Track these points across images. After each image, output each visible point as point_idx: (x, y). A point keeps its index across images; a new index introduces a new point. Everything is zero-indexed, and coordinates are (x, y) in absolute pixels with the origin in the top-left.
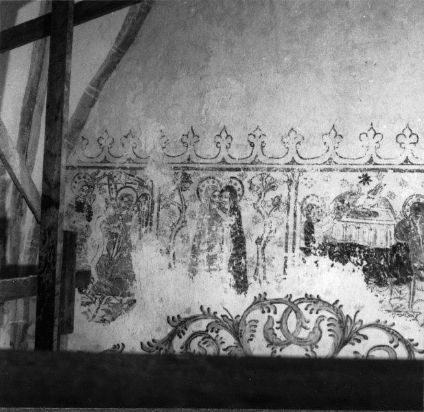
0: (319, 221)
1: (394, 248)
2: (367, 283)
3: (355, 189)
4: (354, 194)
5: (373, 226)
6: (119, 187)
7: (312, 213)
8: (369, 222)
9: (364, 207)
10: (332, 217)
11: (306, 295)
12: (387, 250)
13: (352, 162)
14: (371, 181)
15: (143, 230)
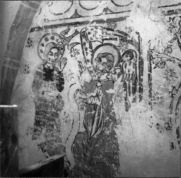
6: (94, 45)
15: (130, 98)
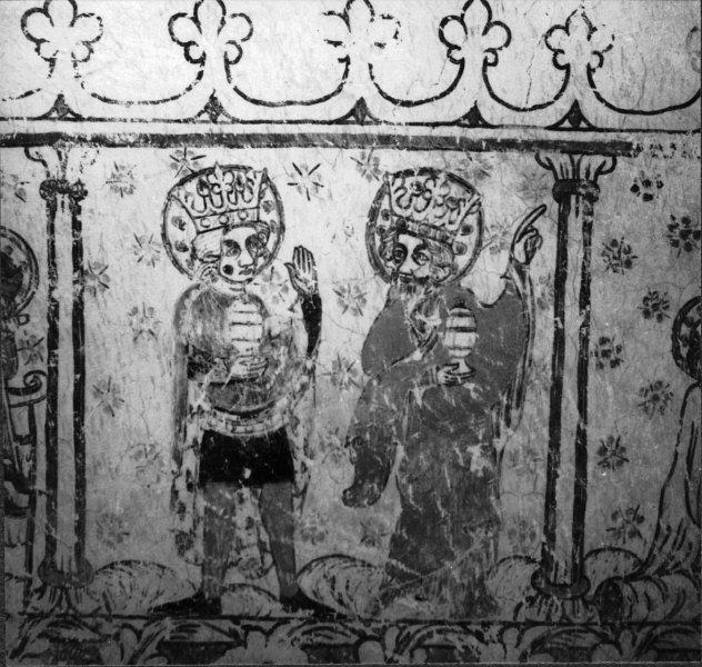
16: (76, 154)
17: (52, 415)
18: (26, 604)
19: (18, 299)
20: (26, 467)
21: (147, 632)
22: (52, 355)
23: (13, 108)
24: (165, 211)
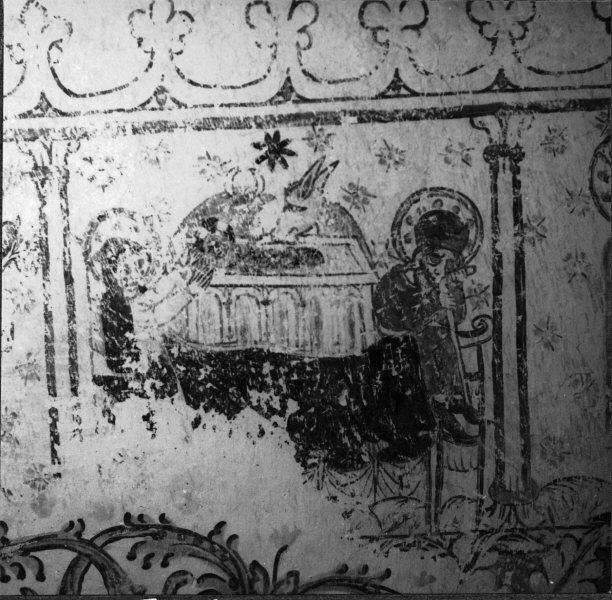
0: (143, 290)
1: (376, 355)
2: (304, 464)
3: (245, 182)
4: (243, 200)
5: (308, 295)
7: (121, 267)
8: (298, 281)
9: (279, 236)
10: (183, 276)
11: (127, 517)
12: (352, 361)
13: (230, 97)
14: (292, 154)
16: (514, 121)
17: (497, 354)
18: (478, 522)
19: (465, 253)
20: (476, 399)
21: (587, 540)
22: (496, 301)
23: (460, 84)
24: (592, 168)
